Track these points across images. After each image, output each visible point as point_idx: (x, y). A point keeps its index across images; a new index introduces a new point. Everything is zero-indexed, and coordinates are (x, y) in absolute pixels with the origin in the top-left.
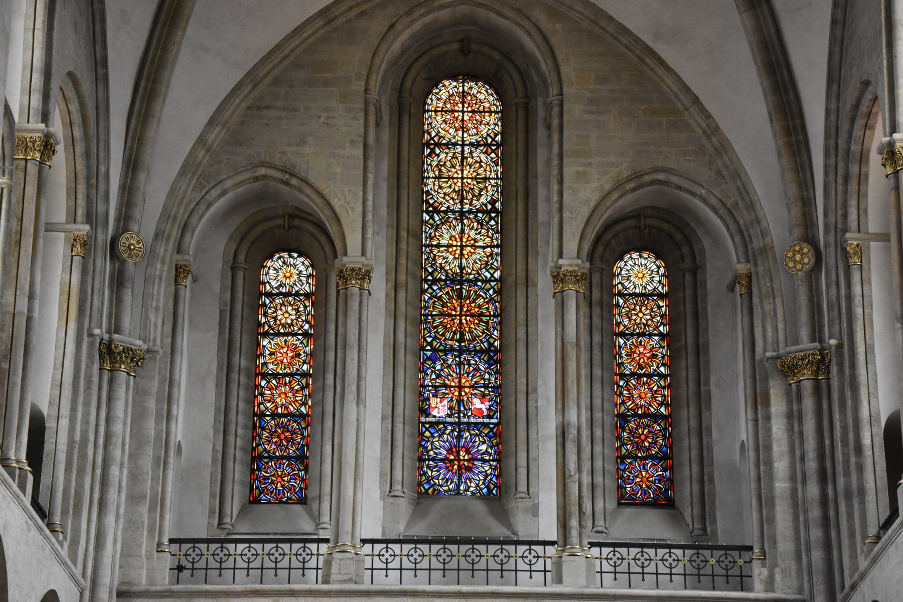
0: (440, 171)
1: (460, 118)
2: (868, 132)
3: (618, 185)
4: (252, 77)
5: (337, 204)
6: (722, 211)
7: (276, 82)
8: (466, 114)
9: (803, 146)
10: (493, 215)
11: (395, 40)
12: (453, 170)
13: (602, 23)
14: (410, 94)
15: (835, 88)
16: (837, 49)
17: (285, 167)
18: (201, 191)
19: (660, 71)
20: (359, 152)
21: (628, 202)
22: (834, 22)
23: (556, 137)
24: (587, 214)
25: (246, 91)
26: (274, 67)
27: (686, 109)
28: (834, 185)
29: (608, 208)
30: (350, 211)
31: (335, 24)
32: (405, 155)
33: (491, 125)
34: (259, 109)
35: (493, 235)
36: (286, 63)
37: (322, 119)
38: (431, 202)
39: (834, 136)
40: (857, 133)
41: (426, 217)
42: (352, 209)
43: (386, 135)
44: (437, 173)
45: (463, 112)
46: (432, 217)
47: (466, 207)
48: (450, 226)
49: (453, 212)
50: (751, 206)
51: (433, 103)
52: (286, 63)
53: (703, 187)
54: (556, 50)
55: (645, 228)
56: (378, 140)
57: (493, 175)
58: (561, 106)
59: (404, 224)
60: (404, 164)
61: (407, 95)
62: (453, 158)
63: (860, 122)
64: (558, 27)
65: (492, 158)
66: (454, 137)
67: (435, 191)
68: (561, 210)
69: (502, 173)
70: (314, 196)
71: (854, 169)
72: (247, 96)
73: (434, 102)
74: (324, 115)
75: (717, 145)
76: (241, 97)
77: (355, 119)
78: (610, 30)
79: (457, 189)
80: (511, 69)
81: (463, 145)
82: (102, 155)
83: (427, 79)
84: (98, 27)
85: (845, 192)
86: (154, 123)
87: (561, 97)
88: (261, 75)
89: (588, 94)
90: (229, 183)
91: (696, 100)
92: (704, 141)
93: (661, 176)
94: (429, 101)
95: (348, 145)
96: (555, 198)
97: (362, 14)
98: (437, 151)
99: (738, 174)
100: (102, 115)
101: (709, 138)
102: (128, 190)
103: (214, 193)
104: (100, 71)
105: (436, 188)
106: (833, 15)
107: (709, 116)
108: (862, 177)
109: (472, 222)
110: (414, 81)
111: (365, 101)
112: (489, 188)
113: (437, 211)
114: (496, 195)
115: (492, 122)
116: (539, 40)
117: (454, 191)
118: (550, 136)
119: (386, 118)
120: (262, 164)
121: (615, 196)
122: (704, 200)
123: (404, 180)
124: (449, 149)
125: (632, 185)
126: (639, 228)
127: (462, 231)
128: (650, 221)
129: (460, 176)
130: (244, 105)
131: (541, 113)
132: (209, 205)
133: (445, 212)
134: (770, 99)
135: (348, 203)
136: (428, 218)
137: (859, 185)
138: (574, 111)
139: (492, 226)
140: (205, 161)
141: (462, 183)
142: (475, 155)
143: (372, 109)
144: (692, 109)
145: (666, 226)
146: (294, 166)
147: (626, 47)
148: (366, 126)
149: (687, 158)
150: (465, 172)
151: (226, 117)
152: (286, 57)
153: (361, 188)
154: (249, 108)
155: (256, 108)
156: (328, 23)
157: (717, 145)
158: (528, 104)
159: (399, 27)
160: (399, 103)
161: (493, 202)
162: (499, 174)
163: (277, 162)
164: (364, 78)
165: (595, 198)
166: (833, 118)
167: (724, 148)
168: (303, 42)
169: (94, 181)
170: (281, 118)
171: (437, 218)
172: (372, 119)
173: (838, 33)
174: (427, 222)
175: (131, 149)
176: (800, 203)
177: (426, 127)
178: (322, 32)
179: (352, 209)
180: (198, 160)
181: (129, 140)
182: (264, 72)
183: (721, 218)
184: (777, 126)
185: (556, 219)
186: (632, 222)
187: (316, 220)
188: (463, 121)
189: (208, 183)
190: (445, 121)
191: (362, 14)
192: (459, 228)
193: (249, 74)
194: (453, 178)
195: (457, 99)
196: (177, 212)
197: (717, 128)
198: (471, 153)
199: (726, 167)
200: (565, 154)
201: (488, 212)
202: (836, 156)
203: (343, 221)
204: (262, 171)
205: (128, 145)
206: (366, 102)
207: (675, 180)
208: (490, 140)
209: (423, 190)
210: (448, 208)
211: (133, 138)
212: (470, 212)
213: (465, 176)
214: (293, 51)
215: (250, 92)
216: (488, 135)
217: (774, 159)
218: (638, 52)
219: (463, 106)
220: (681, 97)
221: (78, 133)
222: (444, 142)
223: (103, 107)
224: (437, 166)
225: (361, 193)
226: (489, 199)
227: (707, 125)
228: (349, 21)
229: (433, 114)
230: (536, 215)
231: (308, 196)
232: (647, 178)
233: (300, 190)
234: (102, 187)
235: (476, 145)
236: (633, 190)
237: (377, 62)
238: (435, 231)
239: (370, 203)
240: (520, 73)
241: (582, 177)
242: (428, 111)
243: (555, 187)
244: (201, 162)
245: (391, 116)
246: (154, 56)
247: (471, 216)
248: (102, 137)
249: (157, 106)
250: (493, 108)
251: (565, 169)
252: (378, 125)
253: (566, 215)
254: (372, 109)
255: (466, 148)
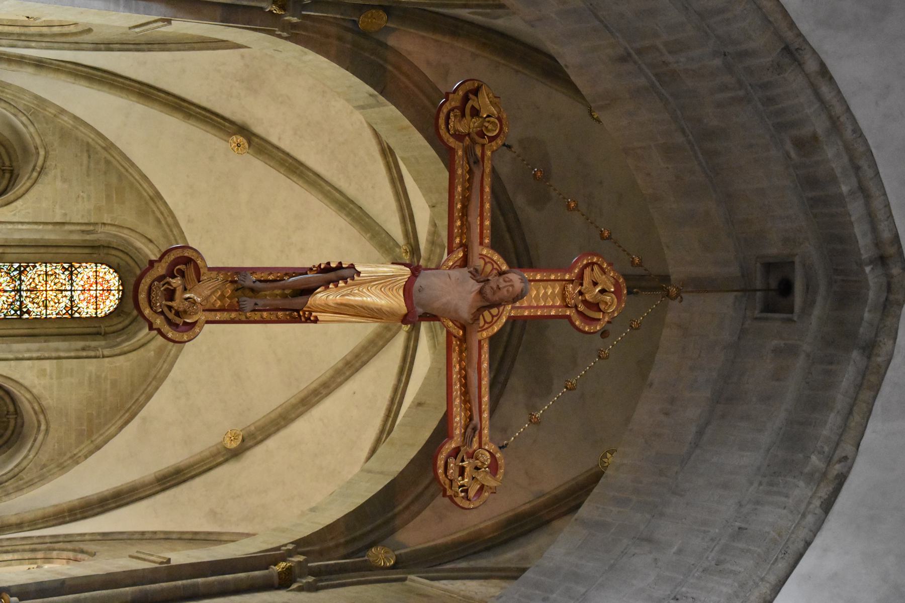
0: (52, 275)
1: (91, 288)
2: (64, 561)
3: (36, 398)
4: (110, 146)
5: (19, 203)
6: (17, 470)
7: (108, 162)
8: (95, 292)
9: (61, 520)
10: (19, 313)
11: (143, 244)
12: (53, 284)
13: (154, 383)
14: (108, 254)
15: (99, 537)
16: (125, 536)
17: (45, 168)
18: (25, 110)
19: (120, 423)
20: (58, 219)
21: (26, 406)
22: (143, 533)
23: (73, 354)
24: (13, 377)
25: (100, 142)
26: (118, 161)
27: (92, 441)
28: (30, 542)
29: (18, 391)
30: (14, 212)
31: (151, 204)
32: (61, 250)
33: (86, 310)
34: (88, 151)
35: (3, 313)
36: (123, 170)
37: (82, 194)
38: (28, 269)
39: (65, 540)
40: (65, 554)
41: (16, 265)
42: (15, 215)
43: (76, 237)
44: (50, 273)
45: (96, 290)
46: (16, 270)
47: (24, 294)
48: (9, 282)
49: (20, 285)
50: (19, 489)
51: (103, 269)
52: (123, 170)
53: (35, 456)
54: (135, 353)
55: (8, 418)
56: (71, 232)
57: (49, 312)
58: (95, 357)
59: (8, 250)
60: (54, 250)
61: (105, 251)
62: (62, 283)
63: (71, 555)
64: (152, 353)
65: (62, 311)
66: (77, 285)
67: (36, 272)
68: (17, 359)
69: (51, 318)
70: (24, 189)
71: (40, 555)
72: (97, 143)
73: (104, 270)
74: (85, 195)
75: (65, 464)
76: (96, 139)
77: (83, 216)
78: (149, 388)
79: (38, 287)
80: (127, 322)
81: (71, 290)
82: (44, 44)
83: (118, 264)
84: (131, 47)
85: (24, 551)
86: (72, 80)
87: (101, 356)
88: (112, 153)
89: (103, 375)
90: (32, 129)
91: (98, 448)
92: (69, 455)
93: (43, 427)
94: (104, 266)
95: (63, 211)
96: (27, 355)
97: (159, 221)
98: (67, 273)
99: (43, 478)
100: (72, 46)
101: (71, 458)
102: (21, 61)
103: (24, 119)
104: (102, 46)
105: (39, 273)
106: (148, 532)
107: (86, 457)
108: (35, 561)
109: (13, 298)
110: (116, 256)
111: (97, 224)
112: (39, 309)
113: (21, 273)
114: (34, 314)
115: (89, 310)
116: (143, 341)
117: (37, 285)
118: (77, 350)
119: (88, 237)
120: (47, 153)
121: (28, 396)
122: (25, 457)
123: (42, 250)
124: (69, 281)
125: (37, 408)
126: (7, 414)
127: (6, 291)
128: (12, 423)
129: (48, 289)
130: (90, 141)
131: (93, 344)
132: (15, 115)
133: (20, 279)
134: (95, 497)
135: (19, 212)
136: (15, 267)
137: (29, 559)
138: (91, 366)
139: (10, 312)
140: (47, 113)
141: (42, 291)
142: (64, 298)
143: (91, 228)
144: (92, 445)
145: (9, 432)
146: (46, 174)
147: (137, 400)
148: (78, 224)
149: (56, 444)
150: (51, 293)
151: (81, 128)
152: (127, 171)
153: (31, 221)
154: (88, 143)
155: (89, 149)
156: (152, 198)
157: (65, 464)
158: (101, 334)
159: (151, 246)
160: (99, 247)
161: (28, 312)
162: (48, 316)
163: (48, 163)
164: (113, 223)
165: (26, 383)
166: (79, 538)
167: (63, 468)
168: (138, 182)
169: (23, 38)
170: (81, 165)
171: (15, 273)
172: (84, 228)
173: (136, 536)
174: (12, 266)
175: (51, 64)
176: (18, 522)
177: (84, 264)
178: (145, 194)
179: (15, 215)
180: (47, 109)
181: (57, 62)
182: (115, 155)
183: (12, 469)
184: (76, 503)
185: (10, 356)
186: (11, 408)
187: (8, 189)
188: (89, 290)
189: (30, 115)
190: (89, 278)
191: (159, 221)
192: (8, 288)
193: (112, 144)
194: (46, 284)
195: (106, 286)
196: (7, 93)
197: (78, 463)
198: (66, 296)
199: (49, 471)
200: (59, 360)
201: (20, 308)
202: (51, 543)
203: (5, 208)
204: (42, 152)
205: (54, 62)
206: (96, 224)
207: (40, 437)
208: (75, 309)
209: (37, 263)
210: (23, 281)
211: (59, 66)
212: (21, 296)
213: (48, 292)
214: (131, 174)
215: (99, 145)
216: (79, 308)
217: (54, 501)
218: (133, 407)
219: (100, 290)
220: (101, 438)
221: (56, 30)
222: (74, 278)
223: (78, 46)
224: (56, 273)
225: (27, 220)
226: (31, 309)
227: (80, 457)
228: (153, 212)
229: (95, 270)
230: (18, 342)
231: (24, 184)
232: (41, 417)
233: (29, 178)
234: (20, 43)
235: (71, 300)
236: (33, 408)
237: (126, 231)
238: (5, 272)
239: (20, 226)
240: (123, 329)
241: (42, 373)
242: (96, 266)
243: (35, 355)
244: (46, 110)
245: (90, 241)
246: (119, 82)
247: (17, 297)
248: (56, 45)
249: (83, 82)
250: (99, 311)
251: (48, 361)
252: (83, 231)
253: (13, 363)
254: (91, 228)
255: (69, 292)
